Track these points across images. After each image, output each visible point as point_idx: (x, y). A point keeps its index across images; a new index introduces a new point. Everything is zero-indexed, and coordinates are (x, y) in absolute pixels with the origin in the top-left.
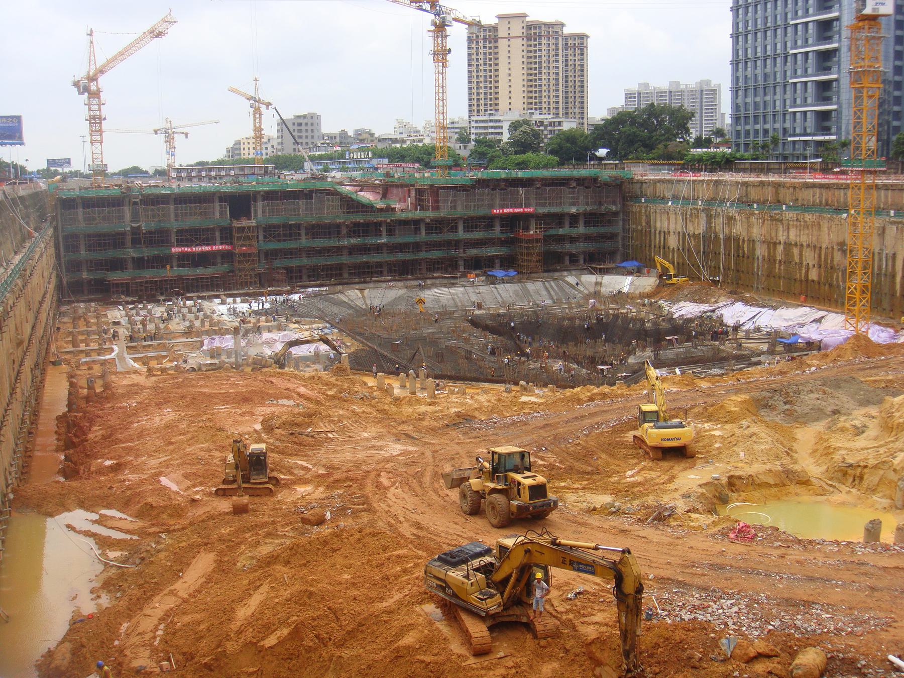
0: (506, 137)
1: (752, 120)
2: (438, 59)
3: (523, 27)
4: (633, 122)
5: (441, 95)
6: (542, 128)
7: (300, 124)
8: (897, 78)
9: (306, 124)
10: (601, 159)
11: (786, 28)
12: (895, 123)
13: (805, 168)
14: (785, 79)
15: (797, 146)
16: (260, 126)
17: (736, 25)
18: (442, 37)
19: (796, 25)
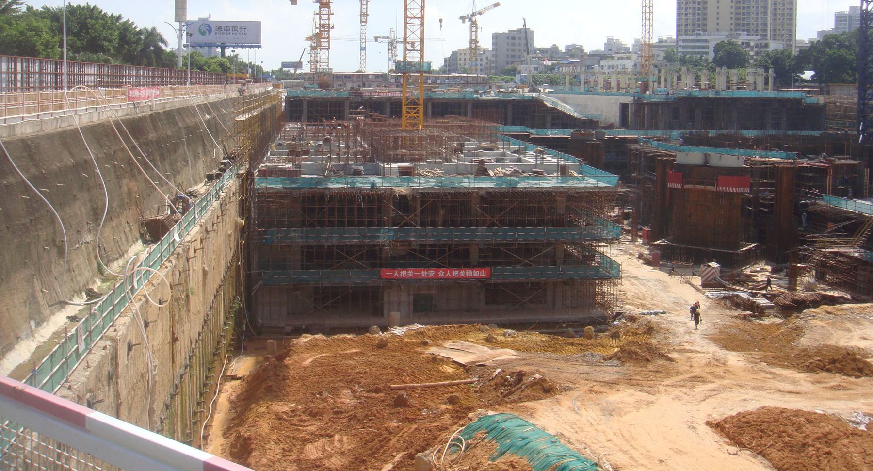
0: (711, 56)
4: (841, 46)
5: (647, 14)
6: (748, 49)
10: (807, 81)
16: (366, 12)
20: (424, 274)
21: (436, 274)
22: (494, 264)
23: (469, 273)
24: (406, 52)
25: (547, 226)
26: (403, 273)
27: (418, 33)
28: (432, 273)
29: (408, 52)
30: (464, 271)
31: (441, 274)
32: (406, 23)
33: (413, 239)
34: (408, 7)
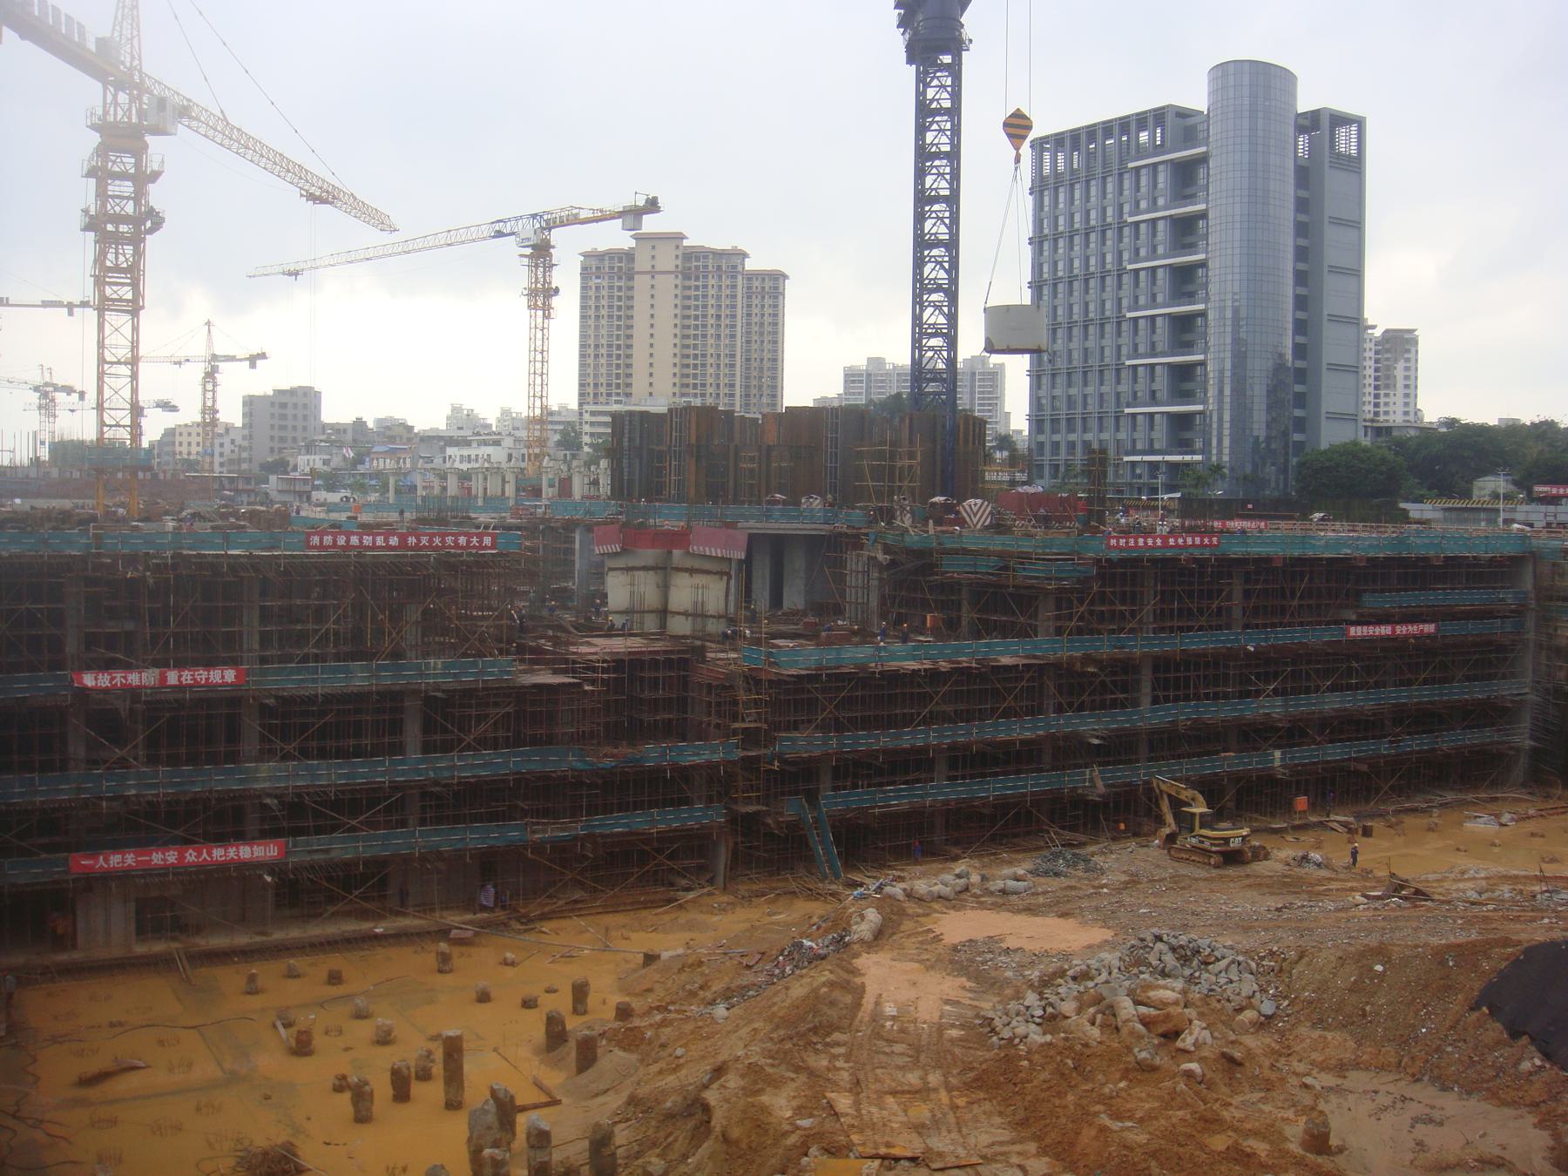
1: (1063, 424)
2: (535, 304)
3: (677, 257)
5: (539, 365)
7: (284, 406)
8: (1300, 364)
9: (295, 406)
11: (1120, 276)
12: (1297, 437)
13: (1155, 508)
14: (1119, 359)
15: (1138, 471)
17: (1037, 267)
18: (544, 267)
19: (1137, 271)
20: (157, 858)
21: (181, 857)
22: (296, 832)
23: (245, 852)
24: (102, 429)
25: (391, 755)
26: (115, 860)
27: (127, 393)
28: (172, 857)
29: (106, 429)
30: (234, 849)
31: (191, 856)
32: (101, 376)
33: (133, 792)
34: (107, 342)
